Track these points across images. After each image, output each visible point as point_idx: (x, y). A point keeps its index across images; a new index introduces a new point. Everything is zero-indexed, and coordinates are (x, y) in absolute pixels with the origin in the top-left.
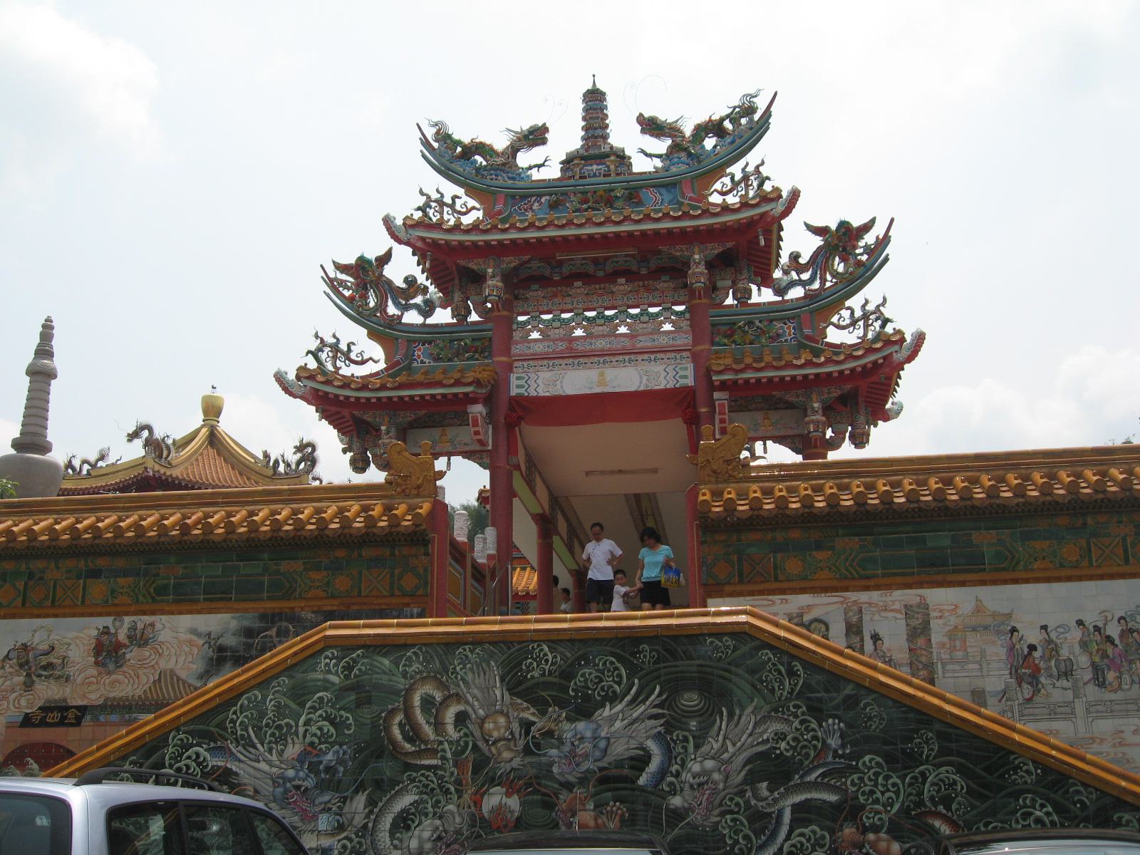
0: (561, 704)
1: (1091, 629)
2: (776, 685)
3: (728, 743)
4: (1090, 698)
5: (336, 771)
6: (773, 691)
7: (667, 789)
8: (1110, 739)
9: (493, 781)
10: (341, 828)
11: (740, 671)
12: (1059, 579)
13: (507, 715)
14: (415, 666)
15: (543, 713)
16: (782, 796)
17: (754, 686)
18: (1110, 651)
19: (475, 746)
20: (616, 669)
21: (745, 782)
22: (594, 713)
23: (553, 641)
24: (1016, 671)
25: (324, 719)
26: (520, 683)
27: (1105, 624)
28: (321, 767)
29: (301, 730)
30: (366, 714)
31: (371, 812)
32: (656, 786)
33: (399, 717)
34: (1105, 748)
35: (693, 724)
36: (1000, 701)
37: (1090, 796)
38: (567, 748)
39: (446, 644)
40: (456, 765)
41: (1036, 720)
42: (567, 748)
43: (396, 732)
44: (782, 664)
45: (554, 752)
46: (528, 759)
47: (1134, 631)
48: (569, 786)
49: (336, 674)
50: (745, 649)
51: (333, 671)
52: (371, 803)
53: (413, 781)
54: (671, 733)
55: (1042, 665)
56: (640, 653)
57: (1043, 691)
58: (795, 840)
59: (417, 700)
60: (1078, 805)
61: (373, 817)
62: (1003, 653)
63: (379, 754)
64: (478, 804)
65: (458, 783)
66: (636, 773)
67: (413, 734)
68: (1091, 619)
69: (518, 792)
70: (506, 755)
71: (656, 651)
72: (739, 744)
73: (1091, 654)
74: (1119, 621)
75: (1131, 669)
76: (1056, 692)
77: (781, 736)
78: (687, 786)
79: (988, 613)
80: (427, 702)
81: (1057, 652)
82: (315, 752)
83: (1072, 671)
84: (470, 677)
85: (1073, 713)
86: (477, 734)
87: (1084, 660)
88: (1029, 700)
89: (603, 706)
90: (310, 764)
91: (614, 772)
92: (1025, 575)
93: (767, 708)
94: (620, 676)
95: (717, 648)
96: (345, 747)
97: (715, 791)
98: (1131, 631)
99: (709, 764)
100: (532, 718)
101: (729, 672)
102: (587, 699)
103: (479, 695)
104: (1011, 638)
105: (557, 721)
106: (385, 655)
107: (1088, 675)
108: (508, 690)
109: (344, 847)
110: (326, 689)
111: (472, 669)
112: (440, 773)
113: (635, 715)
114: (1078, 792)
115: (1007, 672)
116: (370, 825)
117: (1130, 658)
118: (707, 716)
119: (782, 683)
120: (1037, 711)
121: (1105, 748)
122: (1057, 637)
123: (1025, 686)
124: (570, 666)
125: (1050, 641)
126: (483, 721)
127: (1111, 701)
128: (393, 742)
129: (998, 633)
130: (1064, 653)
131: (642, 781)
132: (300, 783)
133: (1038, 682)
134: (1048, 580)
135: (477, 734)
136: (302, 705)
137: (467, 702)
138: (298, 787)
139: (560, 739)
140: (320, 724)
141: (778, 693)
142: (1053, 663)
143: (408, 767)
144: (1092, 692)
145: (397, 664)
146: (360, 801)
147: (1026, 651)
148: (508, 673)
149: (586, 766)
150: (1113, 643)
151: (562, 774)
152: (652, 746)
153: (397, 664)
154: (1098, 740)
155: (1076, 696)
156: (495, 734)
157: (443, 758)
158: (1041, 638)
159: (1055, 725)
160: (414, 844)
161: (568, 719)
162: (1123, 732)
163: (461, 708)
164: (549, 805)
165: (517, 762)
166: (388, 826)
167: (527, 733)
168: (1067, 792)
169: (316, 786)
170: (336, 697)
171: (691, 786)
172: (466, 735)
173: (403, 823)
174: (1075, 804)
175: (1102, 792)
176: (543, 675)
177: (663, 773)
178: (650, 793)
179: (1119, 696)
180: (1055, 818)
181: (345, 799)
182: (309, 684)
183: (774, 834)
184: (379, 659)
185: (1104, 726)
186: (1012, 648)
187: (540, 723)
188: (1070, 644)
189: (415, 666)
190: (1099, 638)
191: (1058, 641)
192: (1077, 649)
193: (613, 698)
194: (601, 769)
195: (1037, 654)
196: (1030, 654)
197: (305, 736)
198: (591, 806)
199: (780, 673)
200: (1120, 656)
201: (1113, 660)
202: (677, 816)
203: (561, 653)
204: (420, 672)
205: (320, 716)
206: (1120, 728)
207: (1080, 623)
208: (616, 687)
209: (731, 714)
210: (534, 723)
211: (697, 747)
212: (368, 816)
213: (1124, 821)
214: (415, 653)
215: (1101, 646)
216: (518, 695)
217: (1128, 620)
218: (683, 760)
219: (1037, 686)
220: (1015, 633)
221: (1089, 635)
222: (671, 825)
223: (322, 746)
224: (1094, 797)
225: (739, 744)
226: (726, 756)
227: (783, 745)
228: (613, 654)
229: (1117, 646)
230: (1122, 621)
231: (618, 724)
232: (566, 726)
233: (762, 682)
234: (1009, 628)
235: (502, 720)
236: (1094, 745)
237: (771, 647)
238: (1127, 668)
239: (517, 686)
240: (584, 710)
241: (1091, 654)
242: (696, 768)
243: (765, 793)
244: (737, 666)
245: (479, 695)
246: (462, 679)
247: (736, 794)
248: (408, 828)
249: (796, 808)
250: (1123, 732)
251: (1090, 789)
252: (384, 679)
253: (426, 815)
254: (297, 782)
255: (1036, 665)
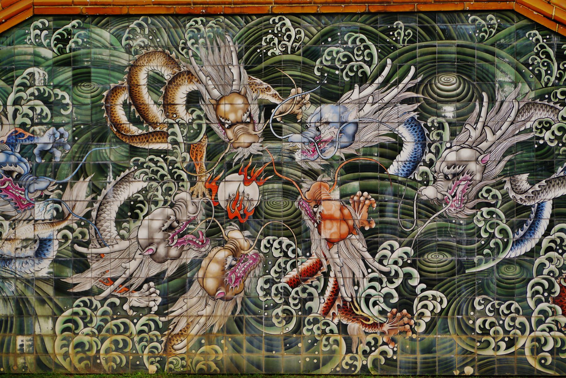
0: (305, 84)
2: (543, 69)
3: (487, 130)
5: (53, 156)
6: (539, 76)
7: (419, 179)
9: (229, 167)
10: (60, 217)
11: (503, 53)
13: (245, 96)
14: (140, 40)
15: (284, 94)
16: (543, 189)
17: (518, 69)
19: (209, 130)
20: (367, 47)
21: (504, 173)
22: (342, 95)
23: (298, 15)
25: (37, 98)
26: (259, 61)
28: (36, 151)
29: (10, 110)
30: (86, 93)
31: (94, 199)
32: (407, 176)
33: (124, 96)
35: (449, 111)
38: (311, 133)
39: (176, 16)
40: (188, 149)
42: (311, 133)
43: (121, 115)
44: (551, 46)
45: (296, 137)
46: (269, 145)
48: (312, 174)
49: (49, 47)
50: (512, 28)
51: (45, 43)
52: (95, 190)
53: (141, 166)
54: (426, 119)
56: (394, 30)
58: (554, 235)
59: (142, 78)
61: (96, 205)
63: (101, 138)
64: (212, 191)
65: (191, 169)
66: (385, 161)
67: (139, 116)
69: (257, 180)
70: (244, 139)
71: (413, 29)
72: (499, 133)
77: (546, 126)
78: (441, 176)
80: (155, 82)
82: (28, 134)
84: (202, 53)
86: (212, 116)
89: (352, 88)
90: (23, 147)
91: (362, 160)
93: (532, 95)
94: (370, 55)
95: (479, 28)
96: (62, 129)
97: (471, 183)
99: (466, 153)
100: (273, 100)
101: (493, 54)
102: (334, 80)
103: (213, 73)
105: (301, 104)
106: (104, 27)
108: (246, 68)
109: (65, 237)
110: (37, 64)
111: (205, 45)
112: (170, 158)
113: (386, 99)
116: (94, 214)
118: (465, 101)
119: (549, 67)
124: (315, 43)
126: (218, 102)
128: (117, 125)
131: (392, 170)
132: (12, 168)
135: (212, 116)
136: (10, 81)
137: (200, 81)
138: (9, 173)
139: (302, 123)
140: (31, 103)
141: (545, 78)
143: (134, 151)
145: (119, 37)
146: (81, 190)
148: (247, 49)
149: (331, 152)
151: (305, 161)
152: (405, 132)
153: (119, 37)
156: (232, 117)
157: (175, 142)
160: (143, 234)
161: (313, 102)
163: (193, 87)
164: (289, 195)
165: (255, 149)
166: (114, 215)
167: (267, 116)
169: (31, 172)
170: (50, 73)
171: (446, 176)
172: (199, 117)
173: (130, 211)
176: (285, 52)
177: (415, 162)
178: (401, 182)
181: (65, 185)
182: (17, 58)
183: (533, 228)
184: (98, 30)
187: (283, 106)
189: (140, 40)
193: (363, 80)
194: (348, 156)
197: (15, 117)
198: (336, 194)
199: (548, 56)
202: (430, 207)
203: (306, 28)
204: (146, 47)
205: (32, 94)
208: (366, 68)
209: (492, 100)
210: (274, 106)
211: (453, 134)
212: (90, 204)
214: (140, 25)
216: (258, 74)
218: (437, 148)
222: (423, 217)
223: (36, 128)
225: (499, 133)
226: (484, 145)
227: (547, 135)
228: (363, 31)
231: (368, 108)
232: (311, 109)
233: (527, 65)
235: (239, 101)
237: (540, 28)
239: (256, 64)
240: (331, 91)
242: (452, 157)
243: (525, 185)
244: (501, 47)
245: (213, 73)
246: (195, 56)
247: (493, 186)
248: (136, 217)
249: (558, 202)
252: (105, 54)
253: (156, 203)
254: (7, 168)
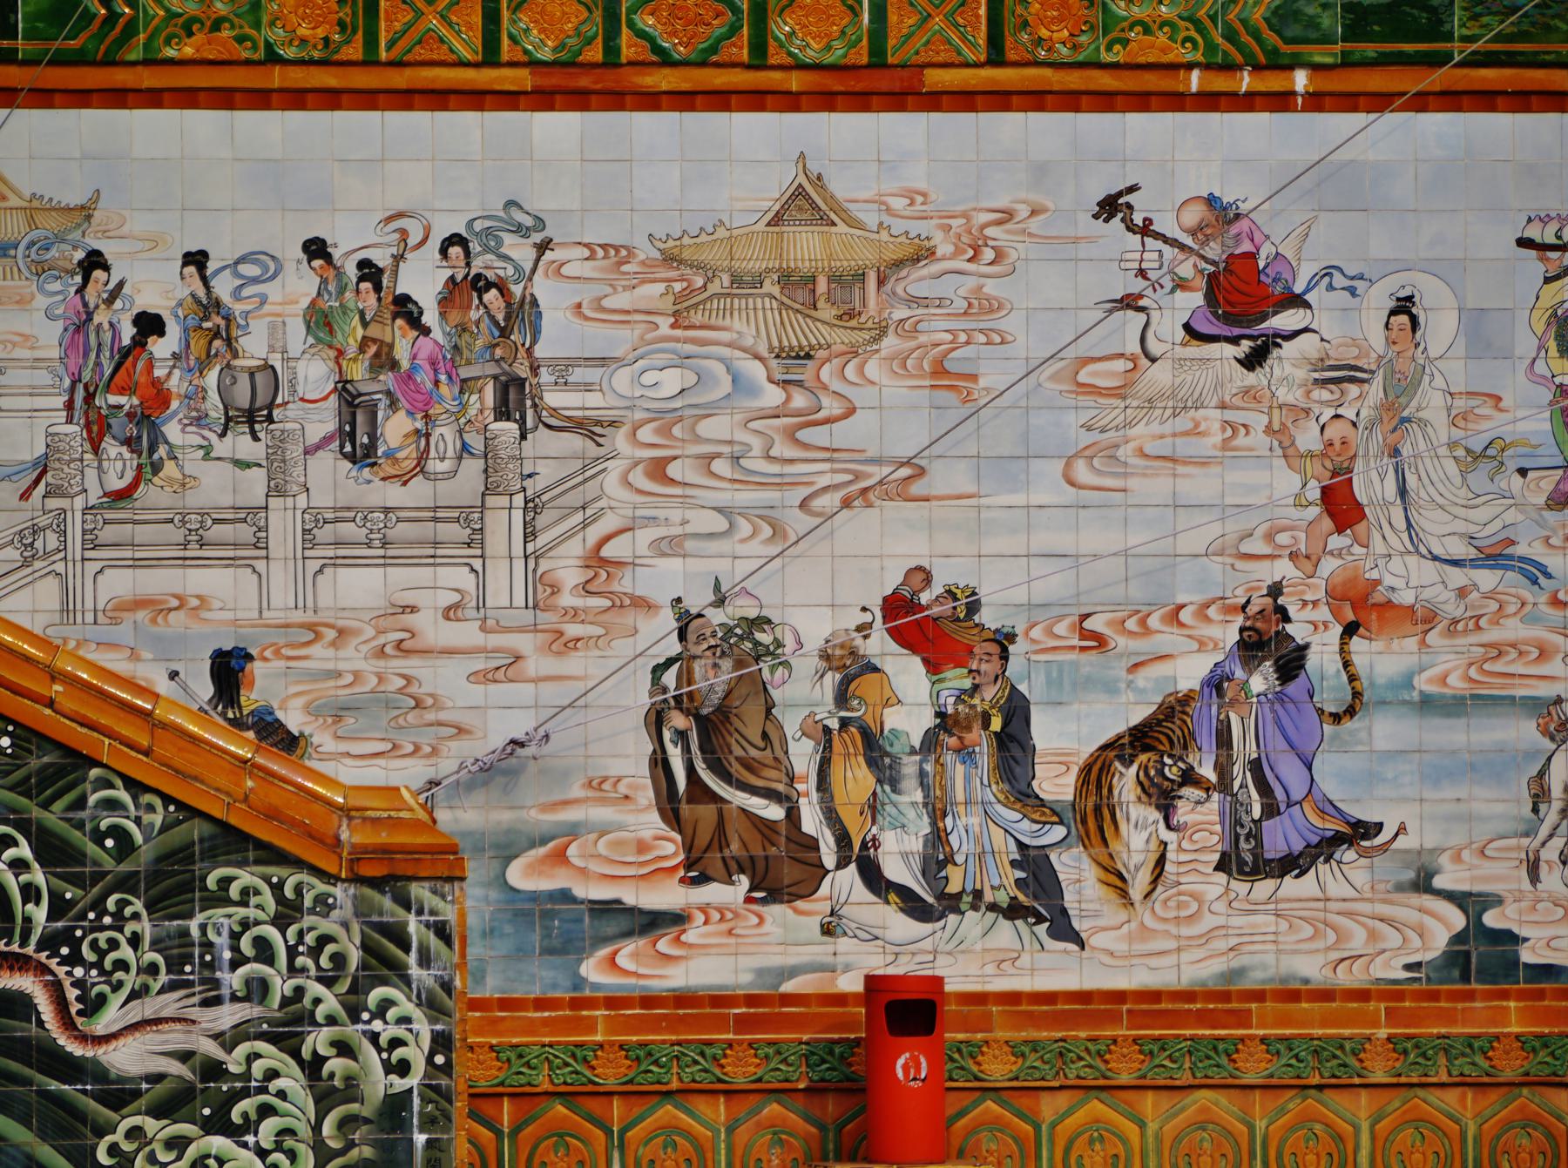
1: (352, 272)
4: (322, 499)
8: (370, 632)
12: (261, 99)
18: (402, 352)
24: (89, 398)
27: (398, 258)
34: (353, 658)
36: (25, 495)
37: (147, 818)
41: (136, 564)
47: (490, 285)
55: (176, 383)
57: (169, 468)
60: (109, 843)
62: (50, 337)
68: (351, 240)
73: (340, 353)
74: (444, 252)
75: (464, 407)
76: (209, 470)
79: (14, 201)
81: (229, 341)
83: (271, 406)
85: (261, 544)
87: (314, 374)
88: (124, 495)
92: (149, 79)
98: (480, 284)
104: (81, 290)
107: (323, 422)
114: (112, 805)
115: (59, 402)
117: (464, 373)
120: (143, 533)
121: (353, 658)
122: (236, 294)
123: (111, 448)
125: (211, 306)
127: (387, 510)
129: (41, 270)
130: (254, 346)
133: (156, 439)
134: (225, 99)
142: (212, 378)
144: (329, 478)
147: (128, 332)
150: (415, 321)
154: (331, 634)
155: (276, 490)
158: (183, 292)
159: (199, 580)
162: (413, 609)
168: (80, 803)
174: (98, 837)
175: (181, 806)
179: (418, 492)
180: (38, 876)
185: (359, 588)
186: (81, 324)
188: (275, 322)
190: (372, 300)
191: (238, 308)
192: (297, 328)
195: (161, 348)
196: (139, 343)
200: (433, 363)
201: (409, 376)
206: (409, 598)
207: (316, 249)
213: (234, 891)
215: (374, 331)
217: (475, 247)
219: (152, 449)
220: (98, 274)
221: (342, 290)
224: (157, 819)
229: (426, 331)
230: (455, 251)
234: (80, 255)
236: (316, 650)
238: (451, 405)
241: (340, 353)
250: (413, 609)
251: (147, 798)
255: (156, 383)
